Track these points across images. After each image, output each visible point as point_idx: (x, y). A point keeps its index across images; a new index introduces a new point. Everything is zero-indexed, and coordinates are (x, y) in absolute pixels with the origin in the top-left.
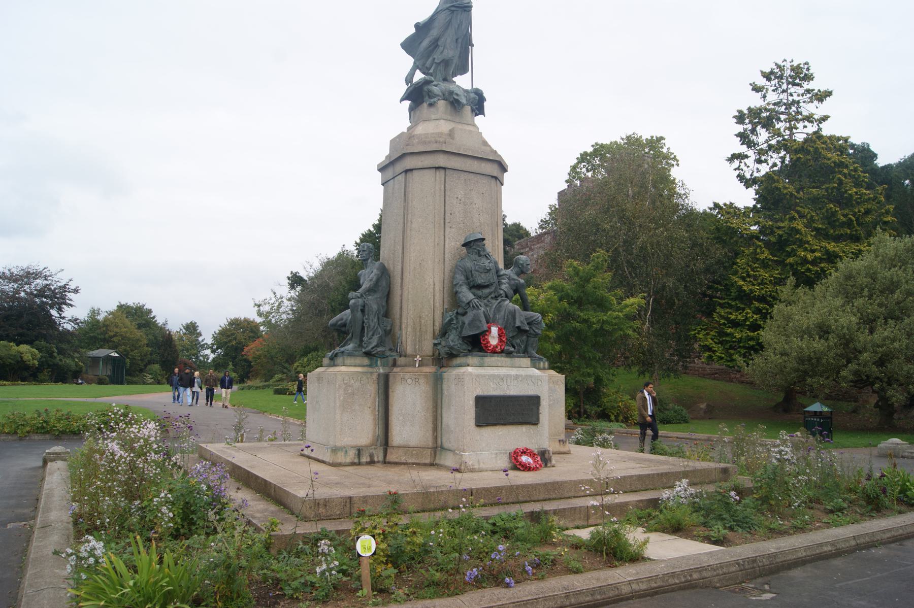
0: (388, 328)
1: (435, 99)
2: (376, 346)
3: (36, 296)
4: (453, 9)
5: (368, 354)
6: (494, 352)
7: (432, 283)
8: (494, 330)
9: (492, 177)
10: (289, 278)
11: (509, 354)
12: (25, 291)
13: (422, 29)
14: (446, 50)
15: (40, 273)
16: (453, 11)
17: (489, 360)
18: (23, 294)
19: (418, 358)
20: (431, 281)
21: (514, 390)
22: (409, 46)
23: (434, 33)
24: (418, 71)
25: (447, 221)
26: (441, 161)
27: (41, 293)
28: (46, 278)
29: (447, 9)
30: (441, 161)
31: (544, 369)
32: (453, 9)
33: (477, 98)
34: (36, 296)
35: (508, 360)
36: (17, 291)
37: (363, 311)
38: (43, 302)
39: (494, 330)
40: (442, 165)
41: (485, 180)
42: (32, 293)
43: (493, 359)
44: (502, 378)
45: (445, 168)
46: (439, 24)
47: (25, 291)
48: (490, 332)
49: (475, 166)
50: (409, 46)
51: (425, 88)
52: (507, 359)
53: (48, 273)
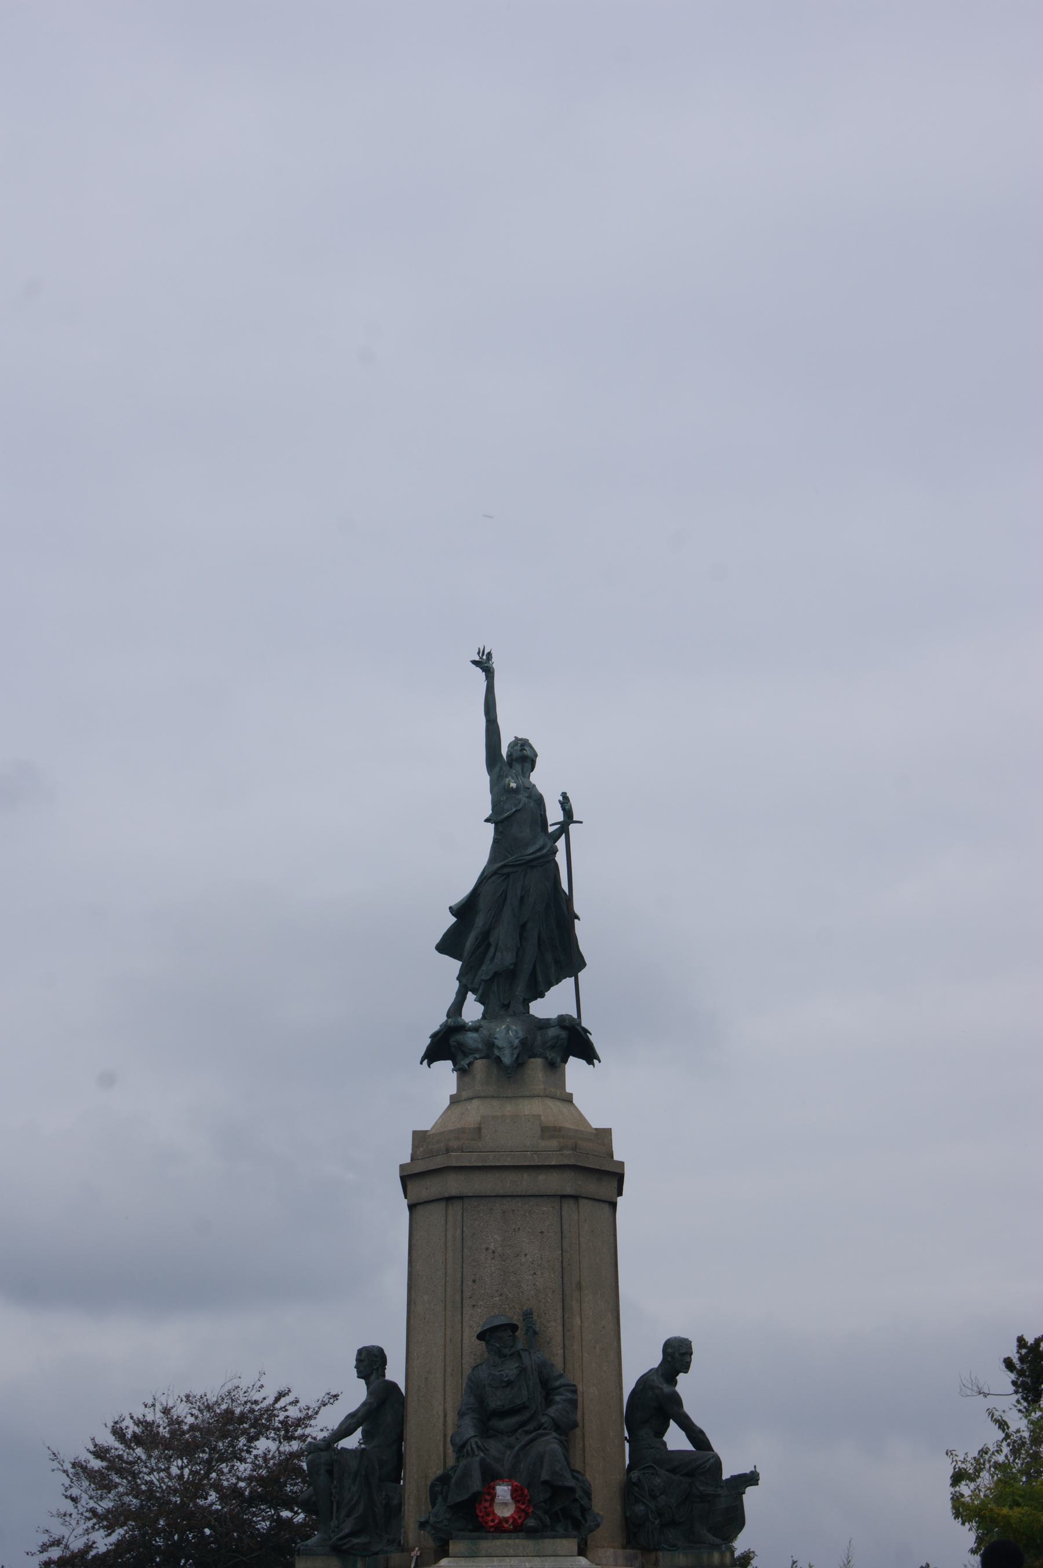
0: (395, 1502)
1: (470, 1059)
2: (353, 1534)
3: (254, 1500)
4: (505, 871)
5: (337, 1550)
6: (500, 1529)
7: (441, 1413)
8: (503, 1491)
9: (563, 1197)
10: (1009, 1364)
11: (533, 1533)
12: (217, 1487)
13: (464, 911)
14: (499, 954)
15: (270, 1412)
16: (508, 875)
17: (485, 1545)
18: (213, 1496)
19: (416, 1552)
20: (441, 1408)
22: (448, 945)
23: (480, 921)
24: (471, 996)
25: (467, 1294)
26: (454, 1185)
27: (271, 1486)
28: (288, 1430)
29: (495, 873)
30: (454, 1185)
32: (505, 871)
33: (564, 1034)
34: (254, 1500)
35: (530, 1544)
36: (194, 1488)
37: (330, 1472)
38: (282, 1524)
39: (503, 1491)
40: (453, 1192)
42: (235, 1490)
43: (498, 1542)
45: (460, 1198)
46: (483, 904)
47: (217, 1487)
48: (493, 1496)
49: (525, 1183)
50: (448, 945)
51: (452, 1041)
52: (526, 1542)
53: (294, 1412)
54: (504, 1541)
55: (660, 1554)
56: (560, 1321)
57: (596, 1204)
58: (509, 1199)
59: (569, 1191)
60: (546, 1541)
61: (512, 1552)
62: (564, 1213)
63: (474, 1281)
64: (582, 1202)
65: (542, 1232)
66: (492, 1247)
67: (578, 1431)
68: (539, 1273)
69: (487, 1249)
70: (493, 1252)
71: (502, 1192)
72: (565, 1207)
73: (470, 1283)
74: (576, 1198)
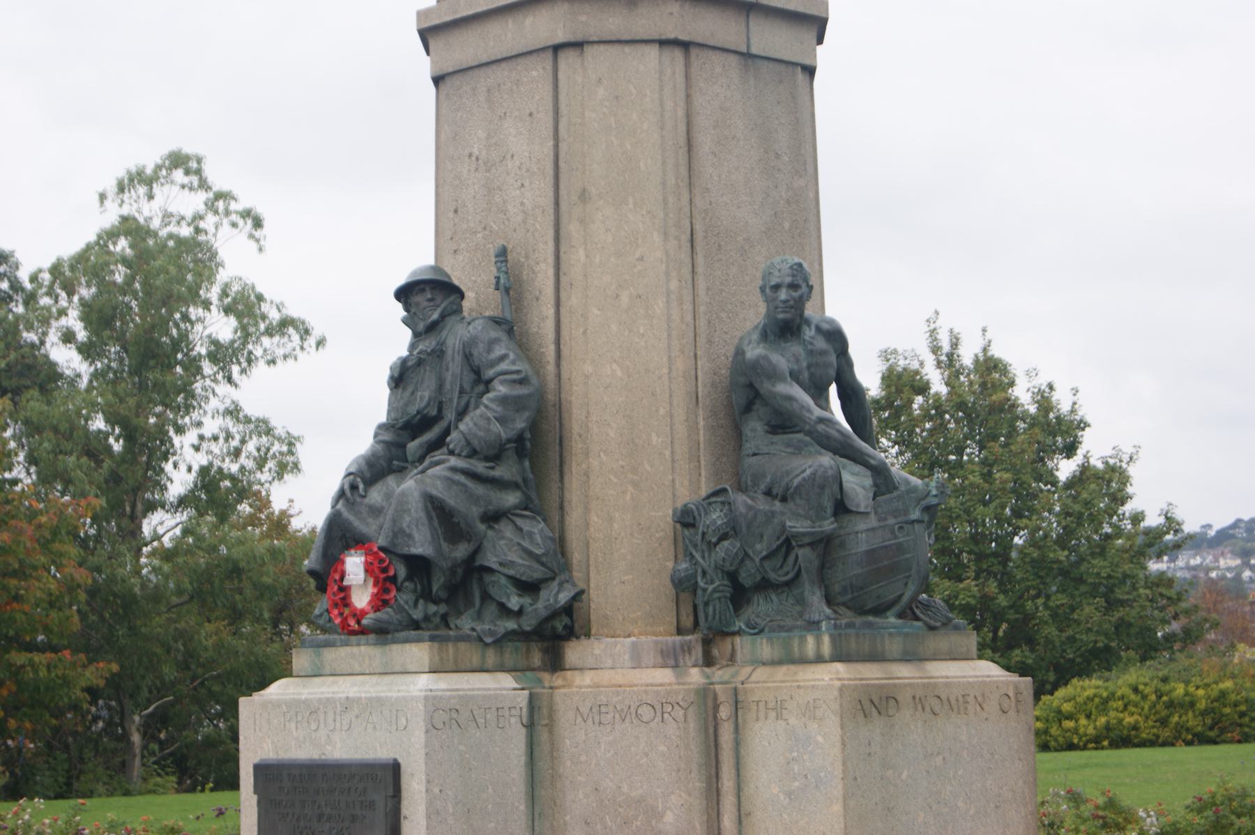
8: (354, 565)
9: (557, 49)
21: (341, 746)
31: (819, 659)
41: (538, 71)
44: (311, 711)
54: (355, 650)
55: (738, 640)
56: (551, 260)
57: (627, 49)
58: (494, 67)
59: (561, 38)
60: (395, 647)
61: (357, 669)
62: (561, 76)
63: (456, 211)
64: (588, 50)
65: (531, 115)
66: (476, 152)
67: (353, 470)
68: (527, 183)
69: (470, 155)
70: (477, 159)
71: (485, 59)
72: (562, 64)
73: (451, 214)
74: (578, 45)
